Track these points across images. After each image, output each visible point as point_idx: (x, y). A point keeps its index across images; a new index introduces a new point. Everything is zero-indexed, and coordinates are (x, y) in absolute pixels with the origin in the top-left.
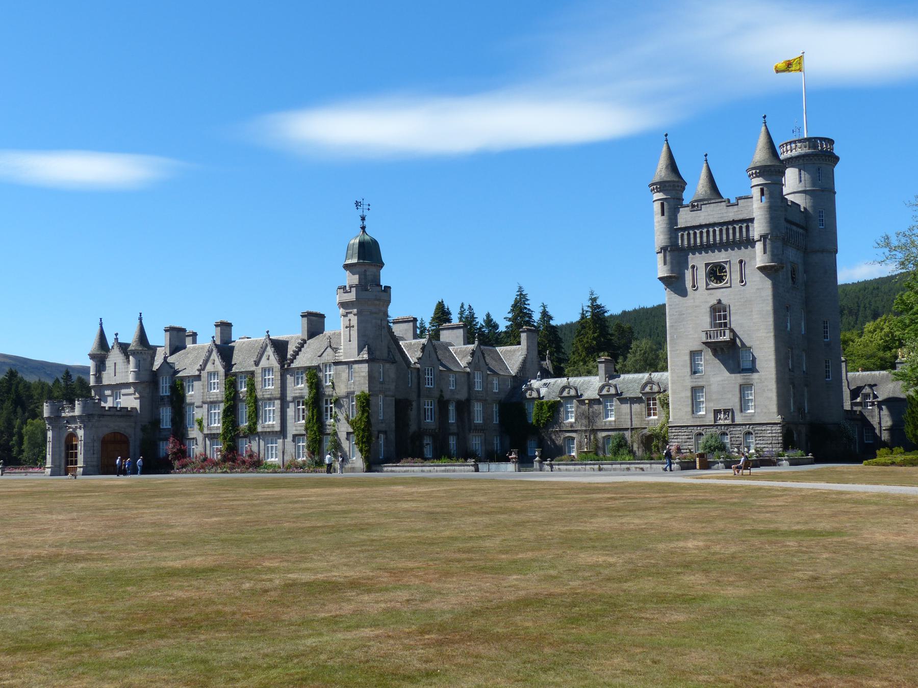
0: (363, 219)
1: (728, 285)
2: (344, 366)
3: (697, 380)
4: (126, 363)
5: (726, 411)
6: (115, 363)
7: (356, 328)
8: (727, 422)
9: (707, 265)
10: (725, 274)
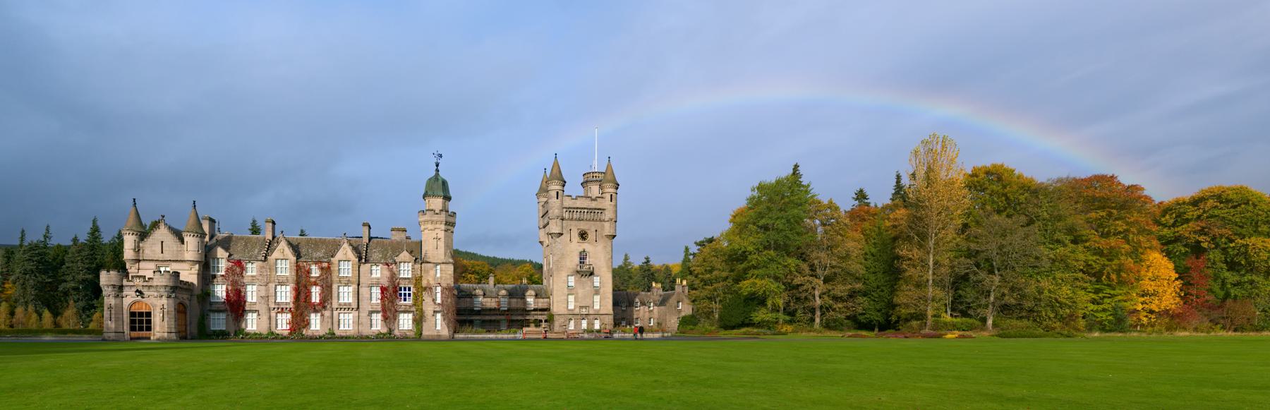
4: (179, 243)
5: (586, 307)
6: (162, 242)
7: (443, 240)
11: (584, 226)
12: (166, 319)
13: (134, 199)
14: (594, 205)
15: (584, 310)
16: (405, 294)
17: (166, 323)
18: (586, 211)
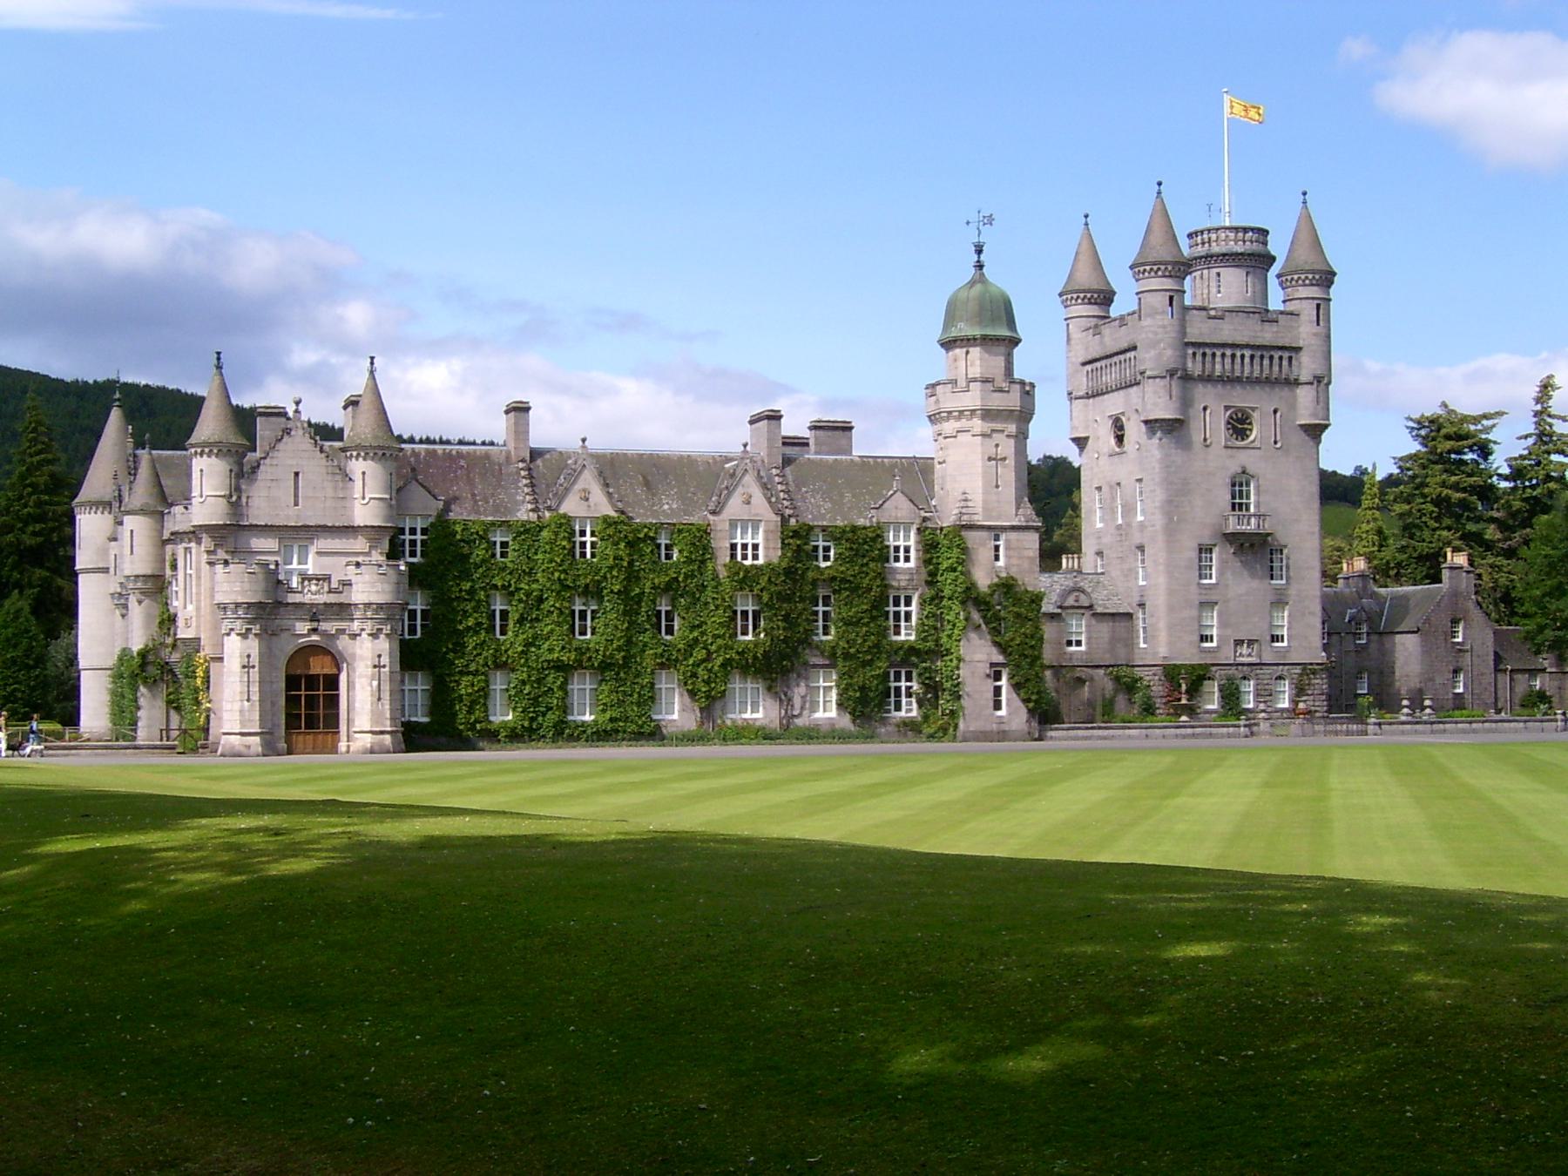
0: (979, 251)
1: (1257, 444)
2: (984, 534)
3: (1209, 592)
5: (1251, 642)
6: (297, 474)
8: (1249, 660)
9: (1227, 408)
10: (1249, 427)
11: (1242, 398)
12: (386, 696)
13: (219, 353)
14: (1267, 335)
15: (1244, 650)
16: (897, 614)
17: (388, 707)
18: (1247, 353)
